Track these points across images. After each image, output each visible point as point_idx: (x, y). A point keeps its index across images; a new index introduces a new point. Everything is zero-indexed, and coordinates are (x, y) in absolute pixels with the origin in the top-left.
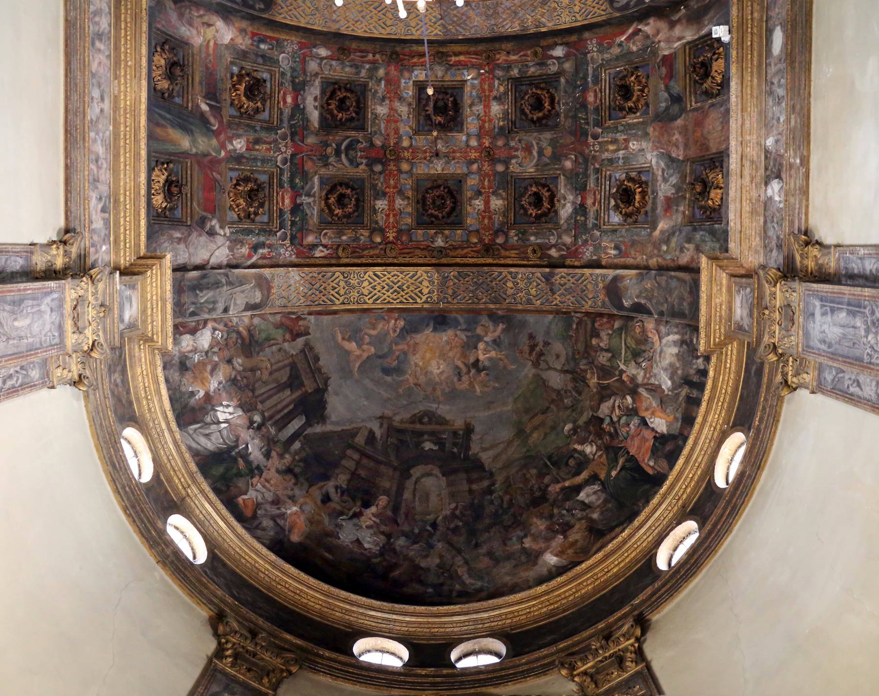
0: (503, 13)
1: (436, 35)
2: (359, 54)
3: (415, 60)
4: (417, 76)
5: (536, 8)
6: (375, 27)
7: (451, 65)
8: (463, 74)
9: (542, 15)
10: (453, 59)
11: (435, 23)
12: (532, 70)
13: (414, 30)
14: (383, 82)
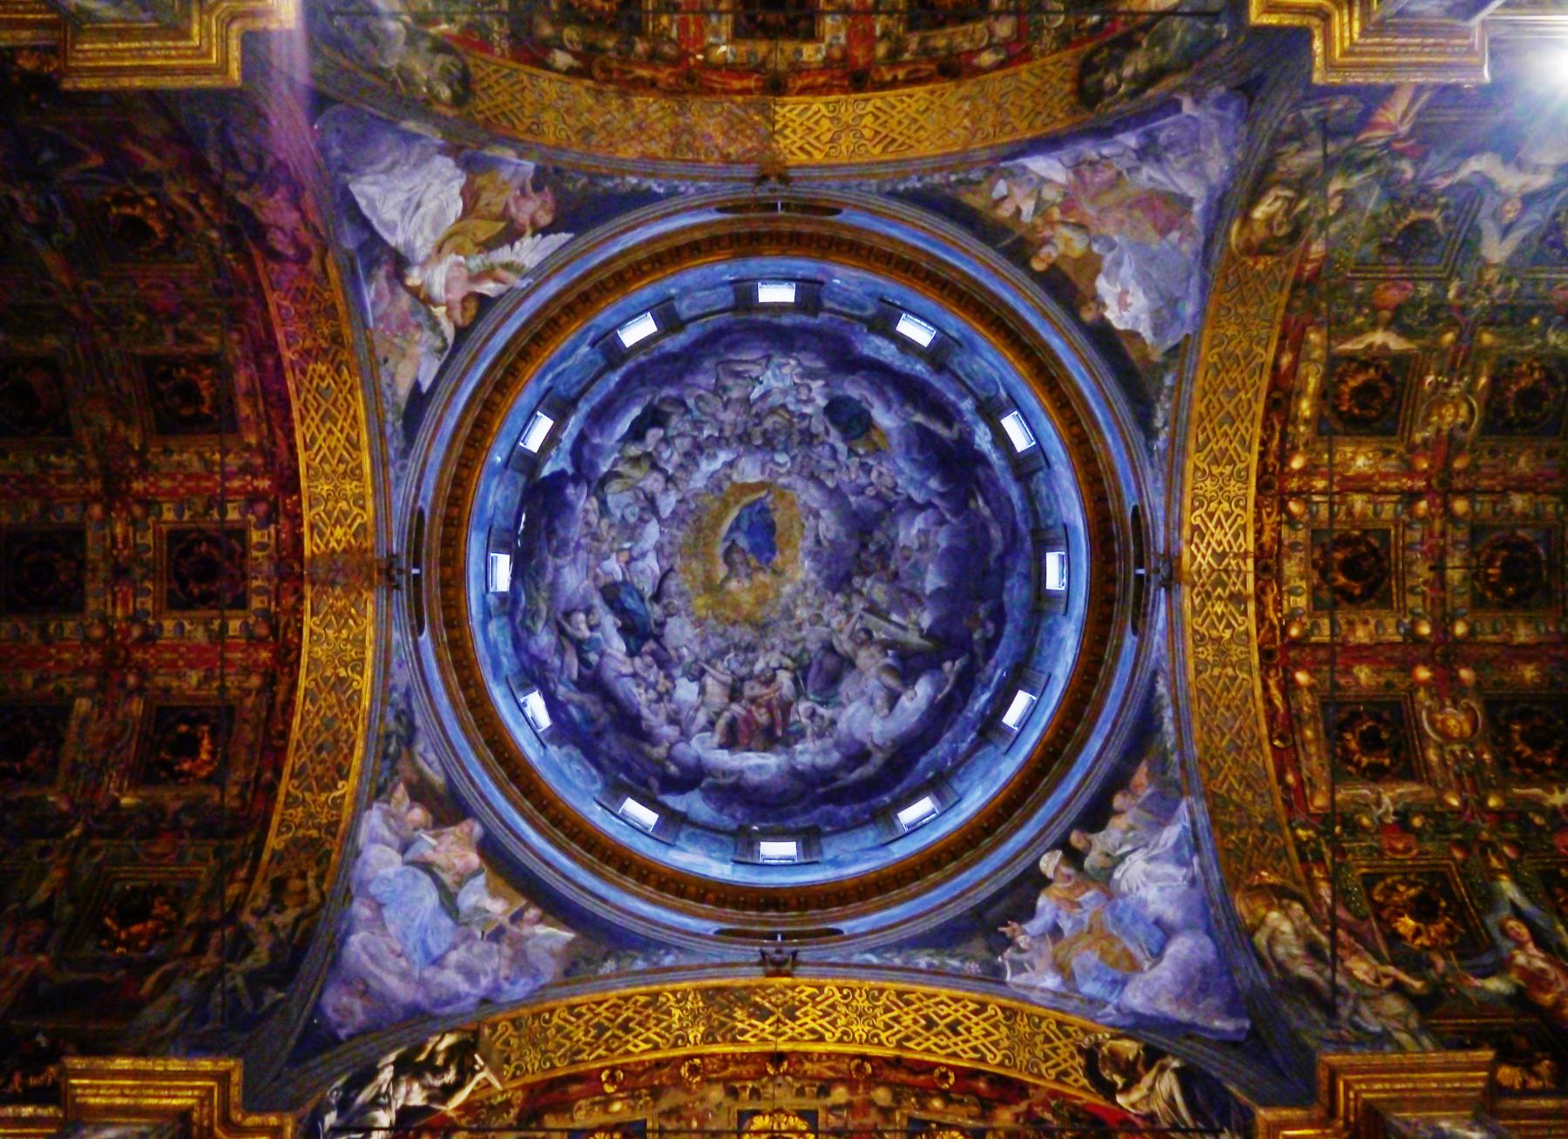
0: (662, 134)
1: (783, 105)
2: (922, 74)
3: (821, 80)
4: (818, 51)
5: (603, 126)
6: (894, 107)
7: (755, 70)
8: (735, 56)
9: (590, 110)
10: (752, 84)
11: (785, 126)
12: (610, 43)
13: (824, 111)
14: (878, 31)
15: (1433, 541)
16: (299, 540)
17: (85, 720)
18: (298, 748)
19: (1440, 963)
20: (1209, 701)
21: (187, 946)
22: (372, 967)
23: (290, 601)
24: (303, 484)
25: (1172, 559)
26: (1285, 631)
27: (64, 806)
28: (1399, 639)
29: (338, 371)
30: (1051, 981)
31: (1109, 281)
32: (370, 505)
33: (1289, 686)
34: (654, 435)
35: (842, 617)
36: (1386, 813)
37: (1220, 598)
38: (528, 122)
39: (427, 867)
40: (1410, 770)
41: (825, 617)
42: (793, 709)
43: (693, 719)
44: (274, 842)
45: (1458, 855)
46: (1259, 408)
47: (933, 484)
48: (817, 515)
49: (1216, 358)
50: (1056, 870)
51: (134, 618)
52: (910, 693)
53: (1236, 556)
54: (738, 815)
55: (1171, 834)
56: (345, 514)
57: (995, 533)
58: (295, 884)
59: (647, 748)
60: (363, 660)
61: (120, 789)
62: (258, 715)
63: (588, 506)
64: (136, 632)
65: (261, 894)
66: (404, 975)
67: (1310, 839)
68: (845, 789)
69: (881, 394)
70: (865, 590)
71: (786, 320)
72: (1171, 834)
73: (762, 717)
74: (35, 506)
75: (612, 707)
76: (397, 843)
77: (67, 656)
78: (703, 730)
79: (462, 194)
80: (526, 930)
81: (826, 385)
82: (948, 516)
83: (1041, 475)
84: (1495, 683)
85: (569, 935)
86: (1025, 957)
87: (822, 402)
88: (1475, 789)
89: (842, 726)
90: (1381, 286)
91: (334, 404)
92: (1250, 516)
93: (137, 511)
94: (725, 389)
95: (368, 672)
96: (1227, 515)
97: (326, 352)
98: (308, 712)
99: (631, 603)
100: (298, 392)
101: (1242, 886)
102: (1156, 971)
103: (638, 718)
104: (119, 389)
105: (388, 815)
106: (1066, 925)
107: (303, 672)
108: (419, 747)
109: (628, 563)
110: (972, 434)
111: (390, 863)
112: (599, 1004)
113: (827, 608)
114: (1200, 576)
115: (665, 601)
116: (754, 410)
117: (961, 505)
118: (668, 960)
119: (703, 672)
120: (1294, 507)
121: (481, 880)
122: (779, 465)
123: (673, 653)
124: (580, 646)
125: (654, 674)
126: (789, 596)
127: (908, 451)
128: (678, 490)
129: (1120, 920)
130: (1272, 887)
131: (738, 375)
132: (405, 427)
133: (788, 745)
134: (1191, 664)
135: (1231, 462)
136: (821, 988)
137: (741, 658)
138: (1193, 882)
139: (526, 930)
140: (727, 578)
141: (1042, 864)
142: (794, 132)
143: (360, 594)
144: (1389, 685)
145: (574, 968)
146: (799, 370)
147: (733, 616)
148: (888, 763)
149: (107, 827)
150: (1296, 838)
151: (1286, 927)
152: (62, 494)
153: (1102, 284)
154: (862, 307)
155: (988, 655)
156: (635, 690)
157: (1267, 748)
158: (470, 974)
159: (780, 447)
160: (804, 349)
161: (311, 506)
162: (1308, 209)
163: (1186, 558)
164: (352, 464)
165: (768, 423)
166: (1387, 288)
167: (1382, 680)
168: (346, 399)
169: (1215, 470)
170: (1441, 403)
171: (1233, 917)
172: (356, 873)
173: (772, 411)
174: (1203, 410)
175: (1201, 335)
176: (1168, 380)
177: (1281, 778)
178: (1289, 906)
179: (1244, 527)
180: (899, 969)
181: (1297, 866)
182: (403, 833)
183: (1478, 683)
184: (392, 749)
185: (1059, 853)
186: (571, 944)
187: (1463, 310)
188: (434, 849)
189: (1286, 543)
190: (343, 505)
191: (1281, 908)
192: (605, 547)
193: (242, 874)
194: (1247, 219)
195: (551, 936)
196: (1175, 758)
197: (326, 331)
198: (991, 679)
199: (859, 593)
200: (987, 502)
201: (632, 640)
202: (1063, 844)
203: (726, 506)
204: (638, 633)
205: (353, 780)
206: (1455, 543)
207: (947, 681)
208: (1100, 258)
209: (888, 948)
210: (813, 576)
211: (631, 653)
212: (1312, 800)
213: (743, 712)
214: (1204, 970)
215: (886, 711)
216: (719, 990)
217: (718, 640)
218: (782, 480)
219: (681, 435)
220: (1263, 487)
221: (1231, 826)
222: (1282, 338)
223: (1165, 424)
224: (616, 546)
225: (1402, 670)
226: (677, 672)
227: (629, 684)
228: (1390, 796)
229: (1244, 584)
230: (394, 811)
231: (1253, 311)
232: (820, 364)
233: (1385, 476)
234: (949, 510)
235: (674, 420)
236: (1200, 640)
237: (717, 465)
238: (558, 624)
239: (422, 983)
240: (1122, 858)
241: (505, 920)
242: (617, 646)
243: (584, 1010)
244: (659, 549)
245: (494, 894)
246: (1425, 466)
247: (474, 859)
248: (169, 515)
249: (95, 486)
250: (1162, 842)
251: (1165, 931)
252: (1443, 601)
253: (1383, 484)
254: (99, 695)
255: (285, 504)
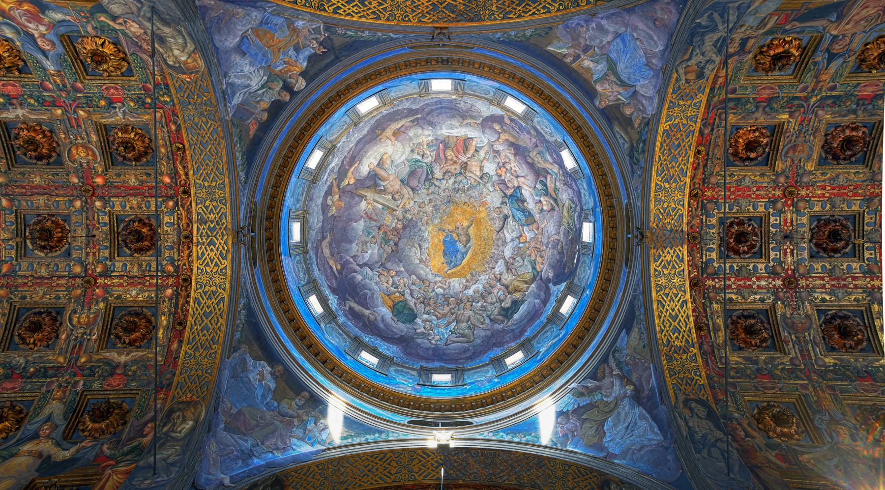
5: (531, 468)
9: (538, 477)
15: (94, 250)
16: (690, 254)
17: (809, 158)
18: (690, 147)
19: (89, 28)
20: (217, 168)
21: (751, 42)
22: (651, 33)
23: (696, 222)
24: (688, 283)
25: (237, 242)
26: (176, 204)
27: (820, 112)
28: (112, 199)
29: (668, 341)
30: (300, 24)
31: (269, 386)
32: (652, 271)
33: (174, 175)
34: (507, 304)
35: (407, 207)
36: (120, 108)
37: (212, 222)
38: (570, 471)
39: (623, 84)
40: (104, 130)
41: (417, 207)
42: (434, 158)
43: (487, 153)
44: (703, 98)
45: (79, 85)
46: (190, 320)
47: (359, 277)
48: (421, 260)
49: (213, 347)
50: (297, 82)
51: (781, 212)
52: (372, 166)
53: (203, 244)
54: (463, 104)
55: (237, 99)
56: (665, 267)
57: (327, 252)
58: (691, 76)
59: (511, 139)
60: (656, 191)
61: (789, 122)
62: (712, 162)
63: (542, 266)
64: (779, 205)
65: (709, 73)
66: (635, 29)
67: (163, 96)
68: (406, 117)
69: (387, 325)
70: (396, 221)
71: (437, 364)
72: (237, 99)
73: (450, 154)
74: (838, 273)
75: (529, 161)
76: (639, 97)
77: (819, 192)
78: (481, 148)
79: (605, 433)
80: (571, 51)
81: (416, 330)
82: (352, 260)
83: (303, 283)
84: (57, 175)
85: (550, 48)
86: (313, 36)
87: (418, 320)
88: (69, 119)
89: (408, 150)
90: (122, 386)
91: (671, 324)
92: (195, 265)
93: (779, 269)
94: (469, 327)
95: (653, 185)
96: (207, 265)
97: (675, 352)
98: (685, 164)
99: (519, 215)
100: (690, 331)
101: (200, 73)
102: (244, 29)
103: (515, 155)
104: (790, 334)
105: (644, 111)
106: (291, 52)
107: (688, 185)
108: (627, 145)
109: (521, 236)
110: (339, 304)
111: (642, 86)
112: (534, 14)
113: (416, 211)
114: (222, 233)
115: (502, 215)
116: (454, 316)
117: (345, 265)
118: (498, 35)
119: (481, 178)
120: (171, 269)
121: (595, 77)
122: (441, 287)
123: (497, 188)
124: (547, 193)
125: (507, 177)
126: (436, 217)
127: (373, 294)
128: (494, 274)
129: (263, 55)
130: (184, 73)
131: (463, 336)
132: (634, 313)
133: (436, 139)
134: (227, 187)
135: (205, 293)
136: (420, 21)
137: (461, 185)
138: (225, 75)
139: (571, 51)
140: (469, 227)
141: (304, 84)
142: (432, 465)
143: (657, 225)
144: (119, 175)
145: (548, 31)
146: (430, 338)
147: (465, 207)
148: (384, 130)
149: (796, 102)
150: (170, 96)
151: (176, 52)
152: (822, 279)
153: (272, 385)
154: (396, 371)
155: (330, 187)
156: (517, 169)
157: (186, 144)
158: (600, 28)
159: (440, 297)
160: (427, 349)
161: (683, 270)
162: (164, 426)
163: (230, 242)
164: (661, 293)
165: (447, 309)
166: (119, 385)
167: (122, 177)
168: (665, 327)
169: (214, 288)
170: (87, 324)
171: (205, 57)
172: (660, 81)
173: (444, 316)
174: (220, 320)
175: (221, 359)
176: (238, 335)
177: (179, 128)
178: (175, 63)
179: (199, 259)
180: (378, 30)
181: (170, 83)
182: (636, 102)
183: (68, 175)
184: (641, 145)
185: (295, 89)
186: (549, 44)
187: (75, 375)
188: (619, 93)
189: (175, 250)
190: (666, 272)
191: (179, 63)
192: (533, 244)
193: (721, 80)
194: (196, 421)
195: (559, 48)
196: (235, 139)
197: (675, 362)
198: (329, 175)
199: (399, 220)
200: (331, 268)
201: (519, 195)
202: (293, 94)
203: (468, 264)
204: (516, 198)
205: (661, 130)
206: (81, 248)
207: (352, 173)
208: (273, 399)
209: (384, 41)
210: (423, 228)
211: (519, 187)
212: (162, 115)
213: (460, 156)
214: (219, 30)
215: (384, 157)
216: (472, 20)
217: (473, 195)
218: (440, 279)
219: (493, 304)
220: (188, 280)
221: (206, 104)
222: (177, 357)
223: (240, 312)
224: (527, 245)
225: (112, 183)
226: (495, 178)
227: (520, 172)
228: (118, 117)
229: (199, 229)
230: (640, 113)
231: (193, 372)
232: (419, 341)
233: (121, 285)
234: (351, 263)
235: (496, 312)
236: (222, 200)
237: (474, 287)
238: (558, 205)
239: (626, 25)
240: (263, 87)
241: (582, 56)
242: (526, 193)
243: (542, 11)
244: (504, 243)
245: (588, 69)
246: (97, 291)
247: (599, 88)
248: (761, 266)
249: (802, 282)
250: (242, 95)
251: (240, 50)
252: (87, 219)
253: (122, 281)
254: (801, 172)
255: (698, 272)
